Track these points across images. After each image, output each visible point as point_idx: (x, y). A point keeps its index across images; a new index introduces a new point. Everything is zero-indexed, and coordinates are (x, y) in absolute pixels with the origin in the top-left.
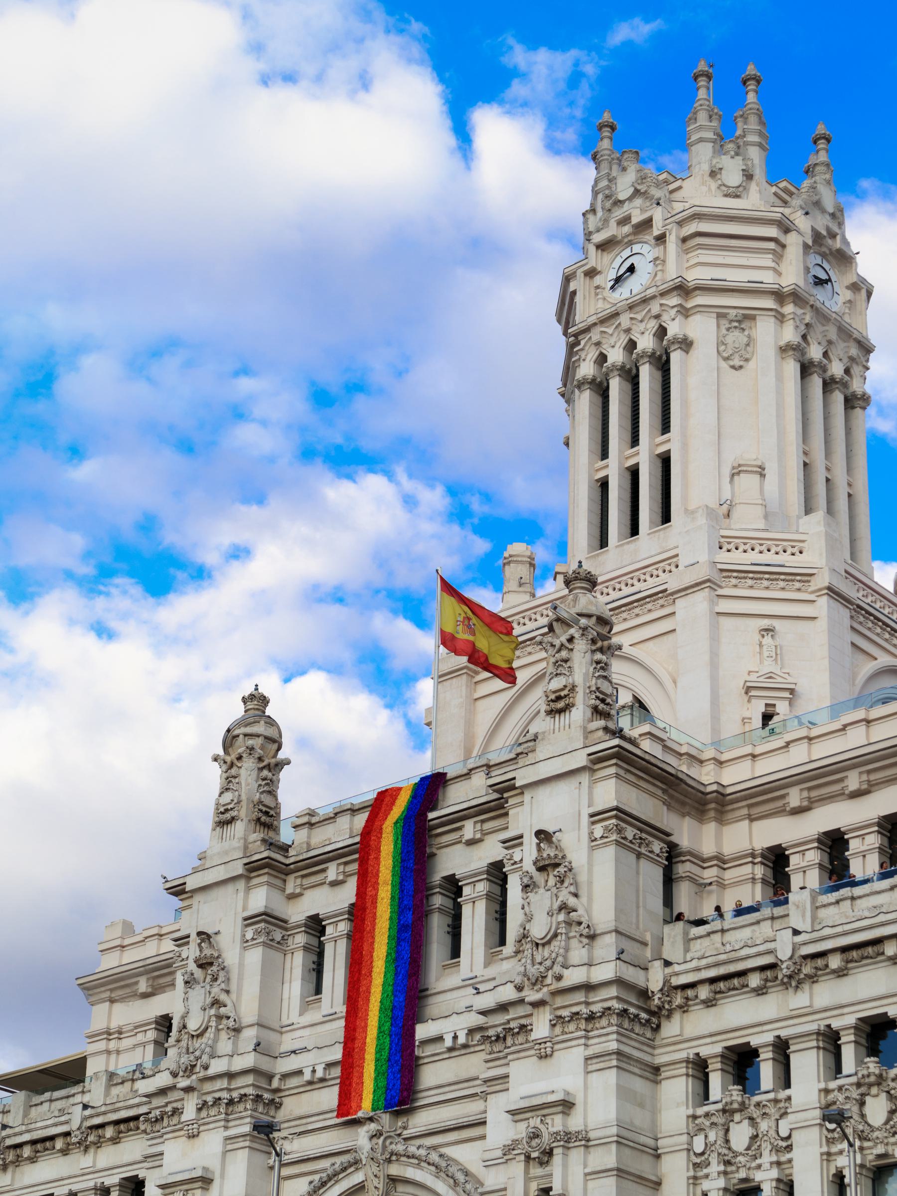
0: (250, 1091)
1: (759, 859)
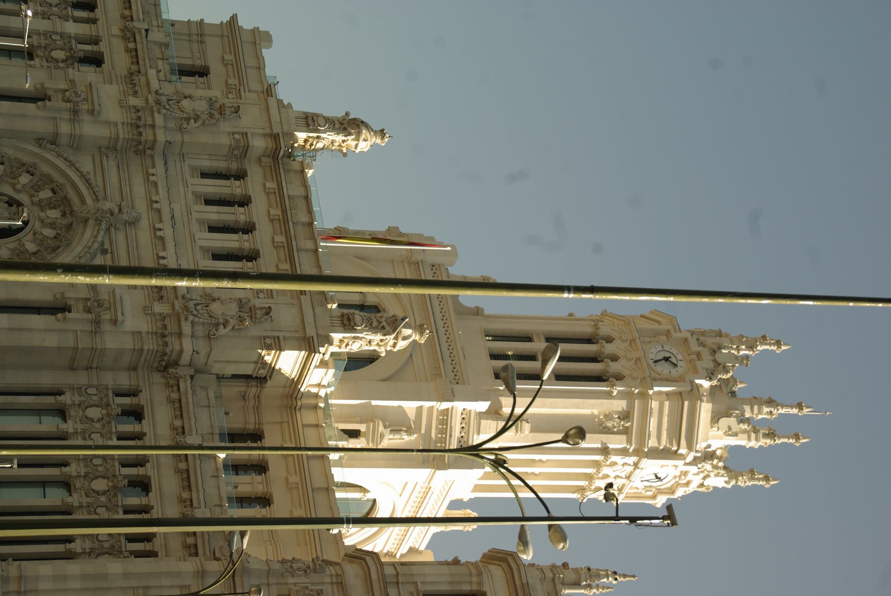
0: (143, 138)
1: (257, 426)
